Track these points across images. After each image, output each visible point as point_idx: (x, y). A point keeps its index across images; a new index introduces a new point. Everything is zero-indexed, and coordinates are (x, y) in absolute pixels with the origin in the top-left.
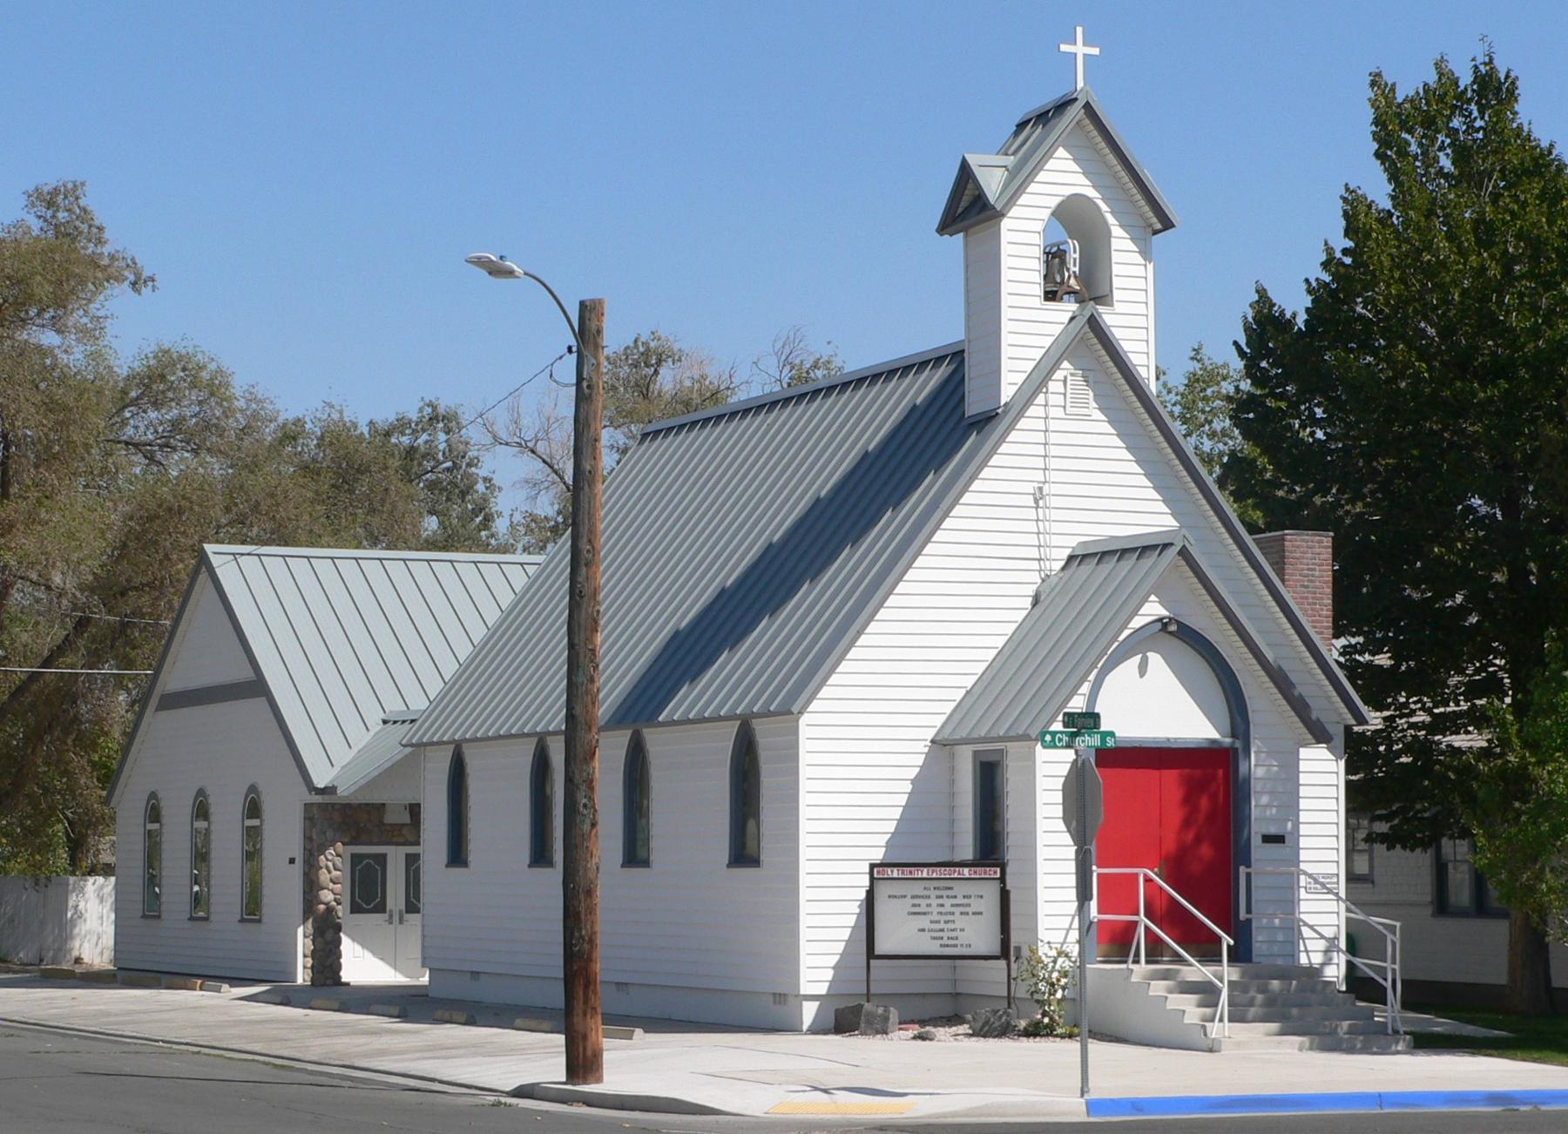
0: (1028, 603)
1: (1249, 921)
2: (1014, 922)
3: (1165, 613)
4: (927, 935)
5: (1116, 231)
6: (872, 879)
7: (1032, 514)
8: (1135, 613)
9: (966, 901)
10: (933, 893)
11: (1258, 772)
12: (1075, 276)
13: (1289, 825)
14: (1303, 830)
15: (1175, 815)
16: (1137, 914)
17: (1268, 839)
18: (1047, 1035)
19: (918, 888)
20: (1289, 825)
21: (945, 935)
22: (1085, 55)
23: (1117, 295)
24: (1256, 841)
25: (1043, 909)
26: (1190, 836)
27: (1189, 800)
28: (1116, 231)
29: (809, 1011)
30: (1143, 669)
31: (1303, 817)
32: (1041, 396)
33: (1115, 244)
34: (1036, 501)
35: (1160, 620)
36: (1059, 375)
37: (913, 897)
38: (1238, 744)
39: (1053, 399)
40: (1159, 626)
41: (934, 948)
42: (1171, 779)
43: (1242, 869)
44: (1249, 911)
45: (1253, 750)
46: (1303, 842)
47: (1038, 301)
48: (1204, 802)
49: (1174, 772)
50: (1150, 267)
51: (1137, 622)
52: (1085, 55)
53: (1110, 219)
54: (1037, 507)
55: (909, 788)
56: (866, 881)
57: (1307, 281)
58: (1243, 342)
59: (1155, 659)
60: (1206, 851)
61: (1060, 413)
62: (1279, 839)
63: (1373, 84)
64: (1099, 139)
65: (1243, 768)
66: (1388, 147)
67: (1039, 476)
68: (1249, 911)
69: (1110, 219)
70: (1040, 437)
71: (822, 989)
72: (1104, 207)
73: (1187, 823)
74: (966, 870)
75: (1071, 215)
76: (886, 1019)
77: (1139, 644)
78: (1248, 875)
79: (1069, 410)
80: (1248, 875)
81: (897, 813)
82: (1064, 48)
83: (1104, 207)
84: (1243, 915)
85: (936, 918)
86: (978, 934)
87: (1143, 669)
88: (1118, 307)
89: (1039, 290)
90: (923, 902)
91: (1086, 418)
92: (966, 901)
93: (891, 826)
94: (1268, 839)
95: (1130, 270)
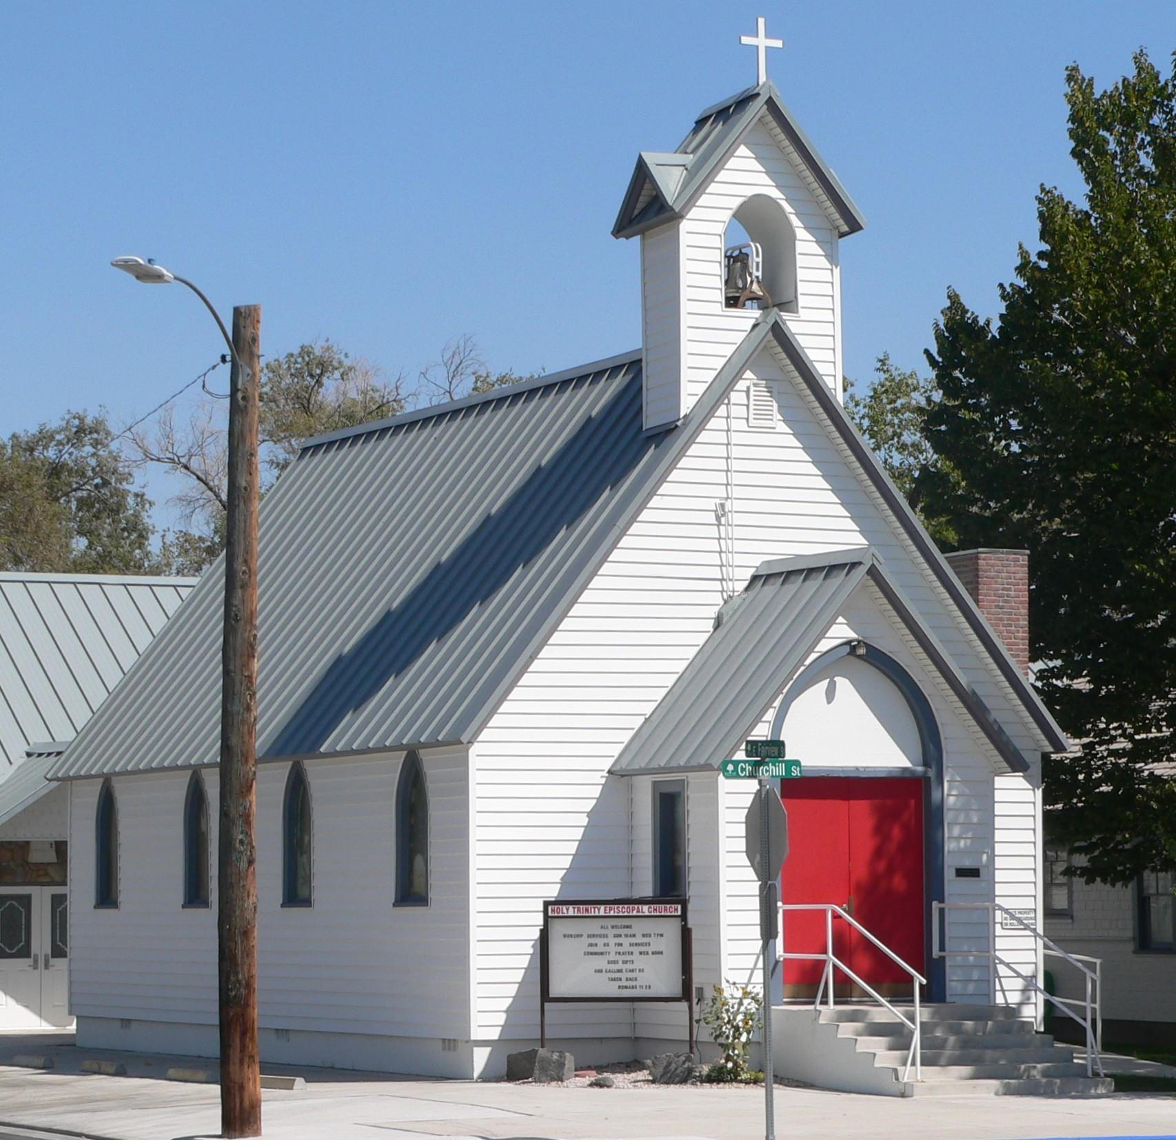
0: (709, 626)
1: (943, 959)
2: (696, 962)
3: (853, 635)
4: (606, 976)
5: (801, 233)
6: (547, 918)
7: (713, 532)
8: (822, 635)
9: (645, 940)
10: (611, 932)
11: (951, 801)
12: (756, 281)
13: (985, 857)
14: (999, 863)
15: (865, 844)
16: (825, 952)
17: (962, 873)
18: (731, 1081)
19: (594, 927)
20: (985, 857)
21: (624, 976)
22: (767, 48)
23: (802, 301)
24: (949, 874)
25: (726, 947)
26: (882, 866)
27: (880, 830)
28: (801, 233)
29: (480, 1058)
30: (830, 695)
31: (999, 849)
32: (723, 407)
33: (800, 247)
34: (718, 518)
35: (848, 643)
36: (741, 385)
37: (589, 936)
38: (932, 773)
39: (735, 411)
40: (847, 648)
41: (612, 990)
42: (862, 809)
43: (935, 904)
44: (942, 948)
45: (946, 779)
46: (999, 876)
47: (719, 308)
48: (896, 832)
50: (837, 271)
51: (824, 645)
52: (767, 48)
54: (719, 524)
55: (584, 820)
56: (539, 920)
57: (1001, 285)
58: (934, 350)
59: (843, 685)
60: (899, 883)
61: (742, 425)
62: (973, 873)
63: (1070, 78)
64: (782, 136)
65: (936, 795)
66: (1085, 146)
68: (942, 948)
70: (722, 451)
71: (494, 1034)
72: (788, 208)
73: (878, 853)
74: (645, 908)
75: (754, 216)
76: (561, 1065)
77: (827, 667)
78: (942, 911)
79: (752, 422)
80: (942, 911)
81: (572, 848)
82: (745, 40)
83: (788, 208)
84: (936, 953)
85: (613, 957)
86: (659, 975)
87: (830, 695)
89: (720, 296)
90: (600, 941)
91: (771, 430)
92: (645, 940)
93: (566, 862)
94: (962, 873)
95: (815, 275)
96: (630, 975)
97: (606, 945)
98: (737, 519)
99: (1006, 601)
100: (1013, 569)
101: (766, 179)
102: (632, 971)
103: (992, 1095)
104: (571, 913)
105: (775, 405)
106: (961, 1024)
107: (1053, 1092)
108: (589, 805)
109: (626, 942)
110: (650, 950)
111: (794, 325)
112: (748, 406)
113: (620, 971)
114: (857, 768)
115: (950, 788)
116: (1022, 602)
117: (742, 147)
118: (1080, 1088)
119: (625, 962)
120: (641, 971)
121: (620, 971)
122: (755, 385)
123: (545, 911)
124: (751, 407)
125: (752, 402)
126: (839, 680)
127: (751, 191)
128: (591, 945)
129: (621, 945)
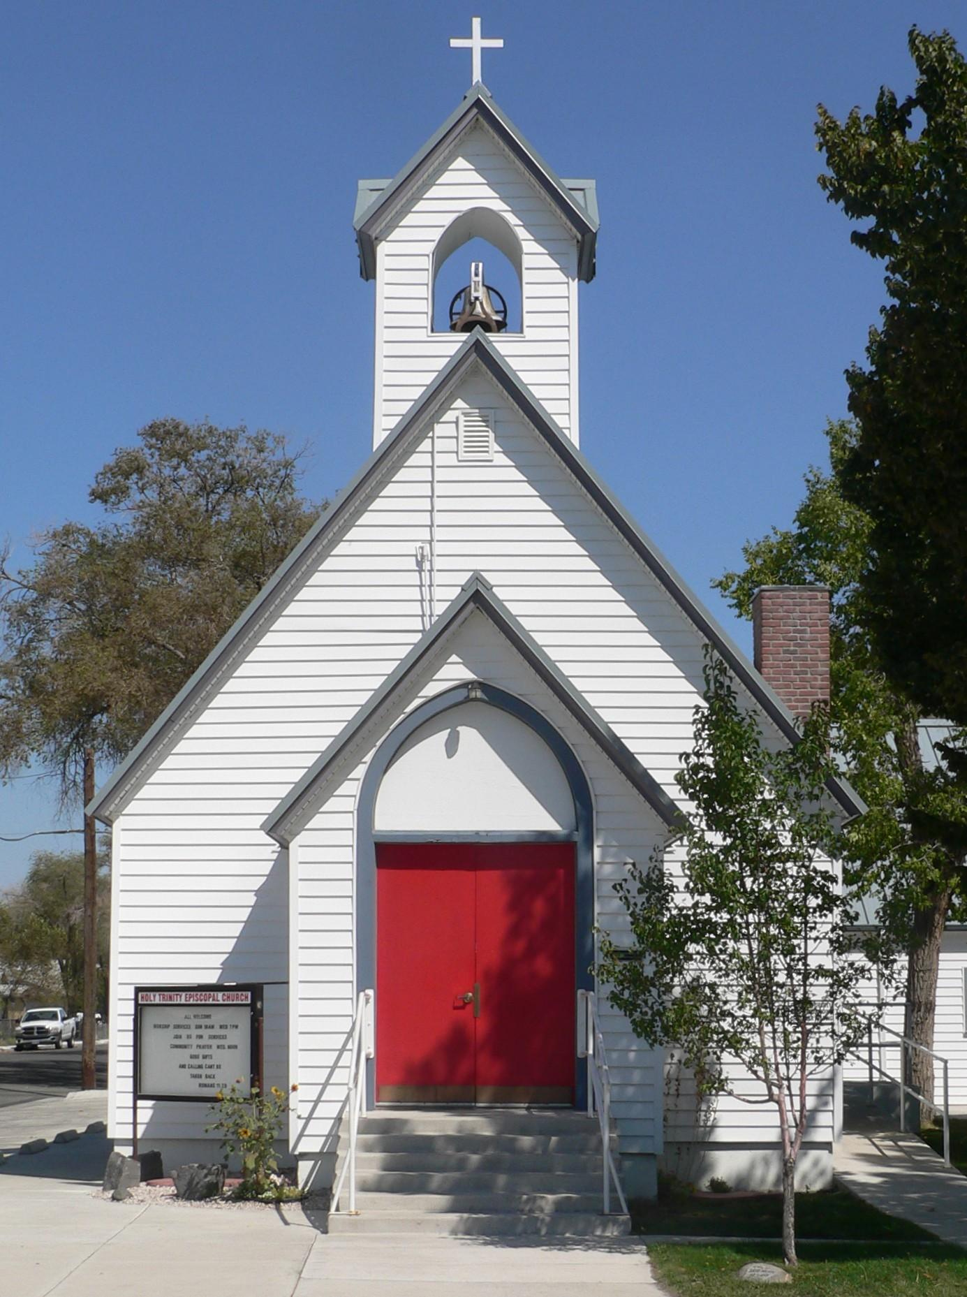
3: (470, 676)
4: (188, 1072)
7: (414, 578)
8: (428, 676)
9: (222, 1032)
15: (497, 922)
19: (178, 1016)
25: (296, 1042)
26: (520, 946)
27: (518, 905)
30: (452, 747)
32: (427, 442)
33: (527, 261)
34: (419, 564)
35: (466, 685)
36: (449, 416)
38: (578, 837)
39: (439, 444)
41: (192, 1088)
47: (423, 334)
48: (539, 907)
49: (495, 875)
51: (431, 689)
53: (522, 233)
54: (421, 571)
55: (251, 899)
59: (469, 736)
60: (543, 966)
65: (582, 863)
67: (425, 534)
69: (522, 233)
72: (512, 219)
73: (514, 932)
81: (237, 930)
82: (455, 43)
83: (512, 219)
85: (195, 1051)
86: (231, 1070)
87: (452, 747)
88: (528, 333)
92: (222, 1032)
93: (229, 945)
96: (209, 1072)
97: (189, 1037)
98: (439, 563)
99: (800, 646)
100: (808, 608)
101: (489, 192)
102: (211, 1067)
103: (445, 1234)
104: (157, 1002)
105: (492, 435)
106: (514, 1140)
107: (537, 1232)
108: (258, 883)
109: (206, 1033)
110: (226, 1043)
111: (501, 344)
112: (457, 438)
113: (200, 1067)
114: (477, 833)
115: (603, 855)
116: (821, 646)
117: (460, 162)
118: (581, 1226)
119: (205, 1057)
120: (219, 1067)
121: (200, 1067)
122: (466, 414)
123: (136, 999)
124: (462, 439)
125: (462, 434)
126: (463, 730)
127: (466, 206)
128: (177, 1037)
129: (201, 1037)
